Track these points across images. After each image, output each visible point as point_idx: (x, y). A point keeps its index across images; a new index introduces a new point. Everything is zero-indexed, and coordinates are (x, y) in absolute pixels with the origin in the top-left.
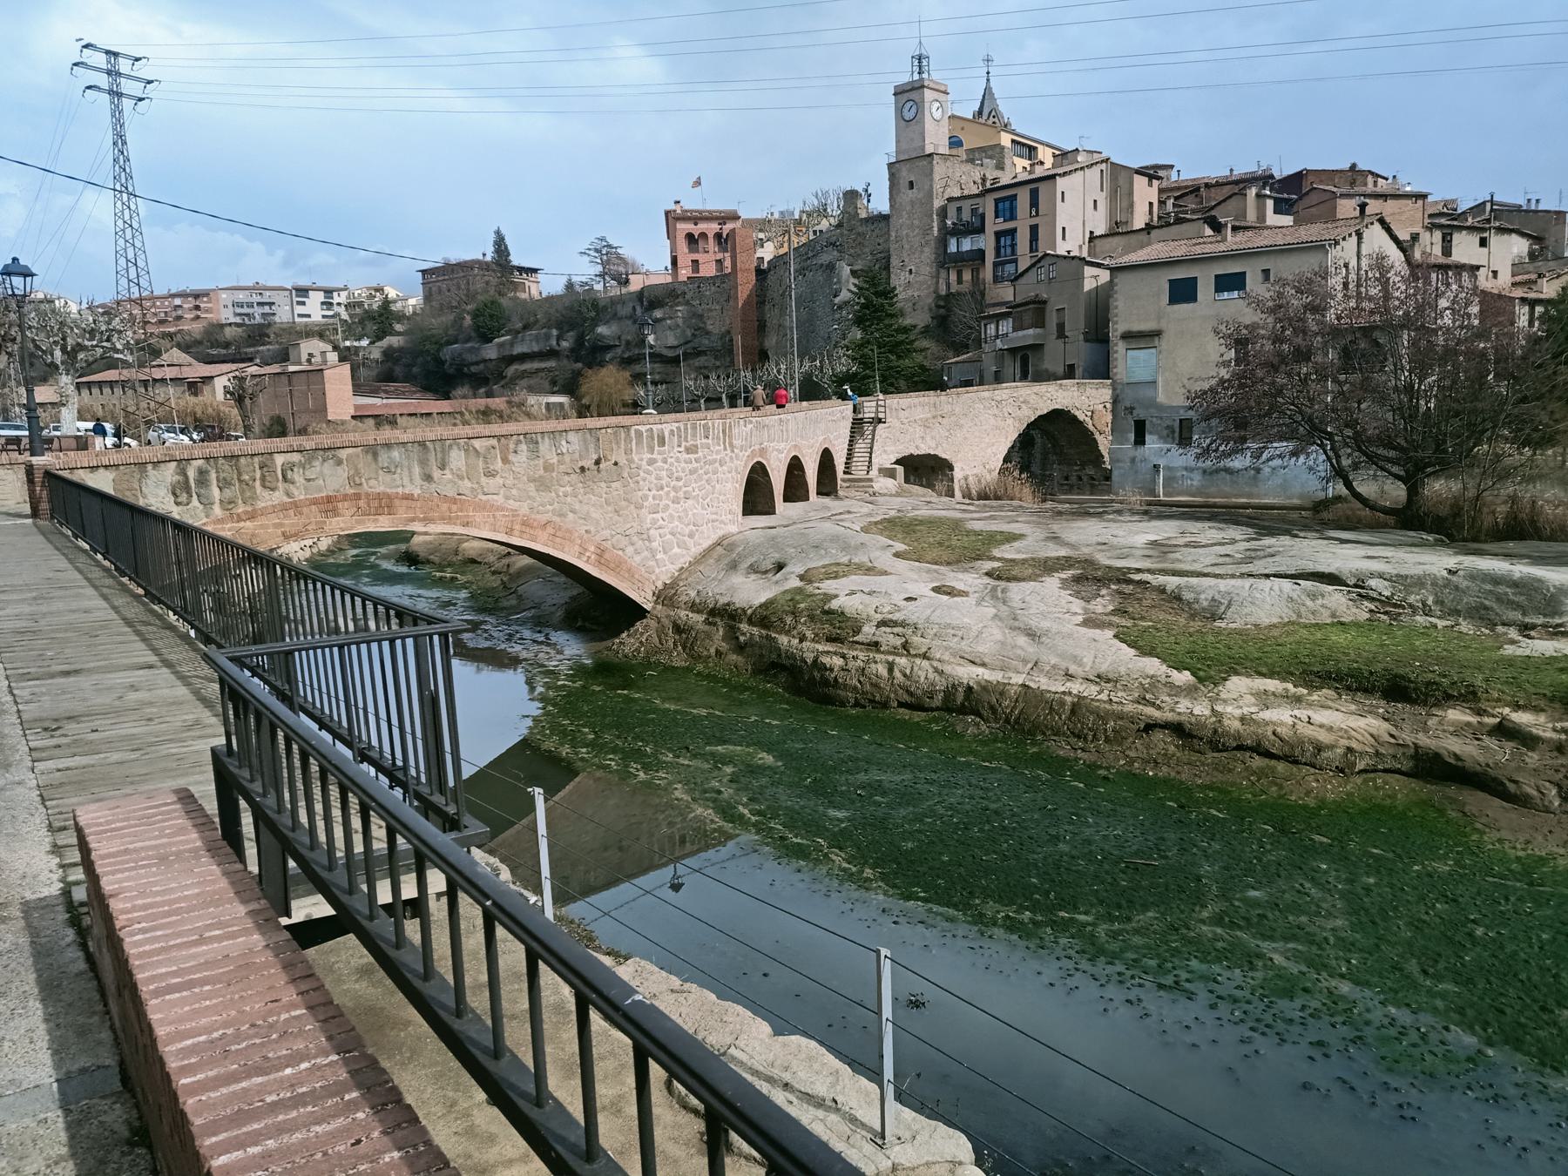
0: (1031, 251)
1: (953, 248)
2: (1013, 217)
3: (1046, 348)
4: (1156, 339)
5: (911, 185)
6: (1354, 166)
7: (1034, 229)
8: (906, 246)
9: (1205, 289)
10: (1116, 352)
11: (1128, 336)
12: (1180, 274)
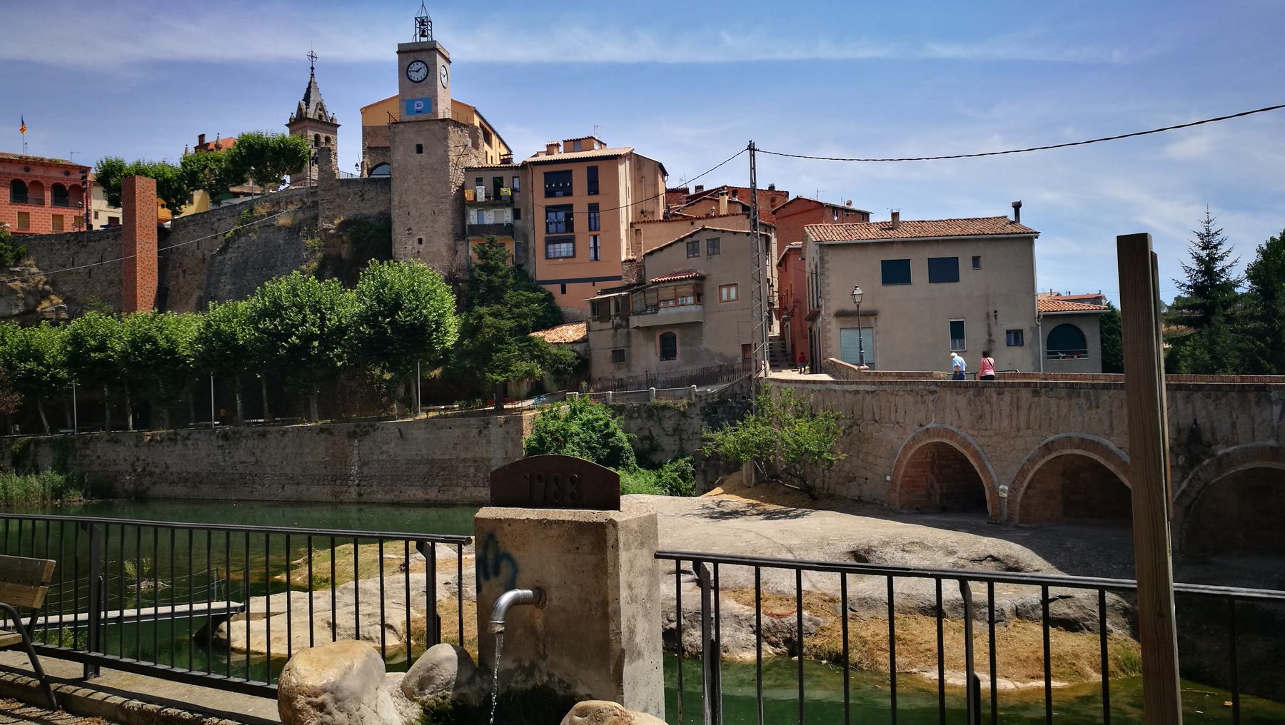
0: (590, 230)
1: (473, 218)
2: (569, 193)
3: (706, 328)
4: (872, 319)
5: (420, 149)
6: (772, 188)
7: (594, 208)
8: (413, 213)
9: (919, 272)
10: (830, 330)
11: (841, 314)
12: (894, 255)
